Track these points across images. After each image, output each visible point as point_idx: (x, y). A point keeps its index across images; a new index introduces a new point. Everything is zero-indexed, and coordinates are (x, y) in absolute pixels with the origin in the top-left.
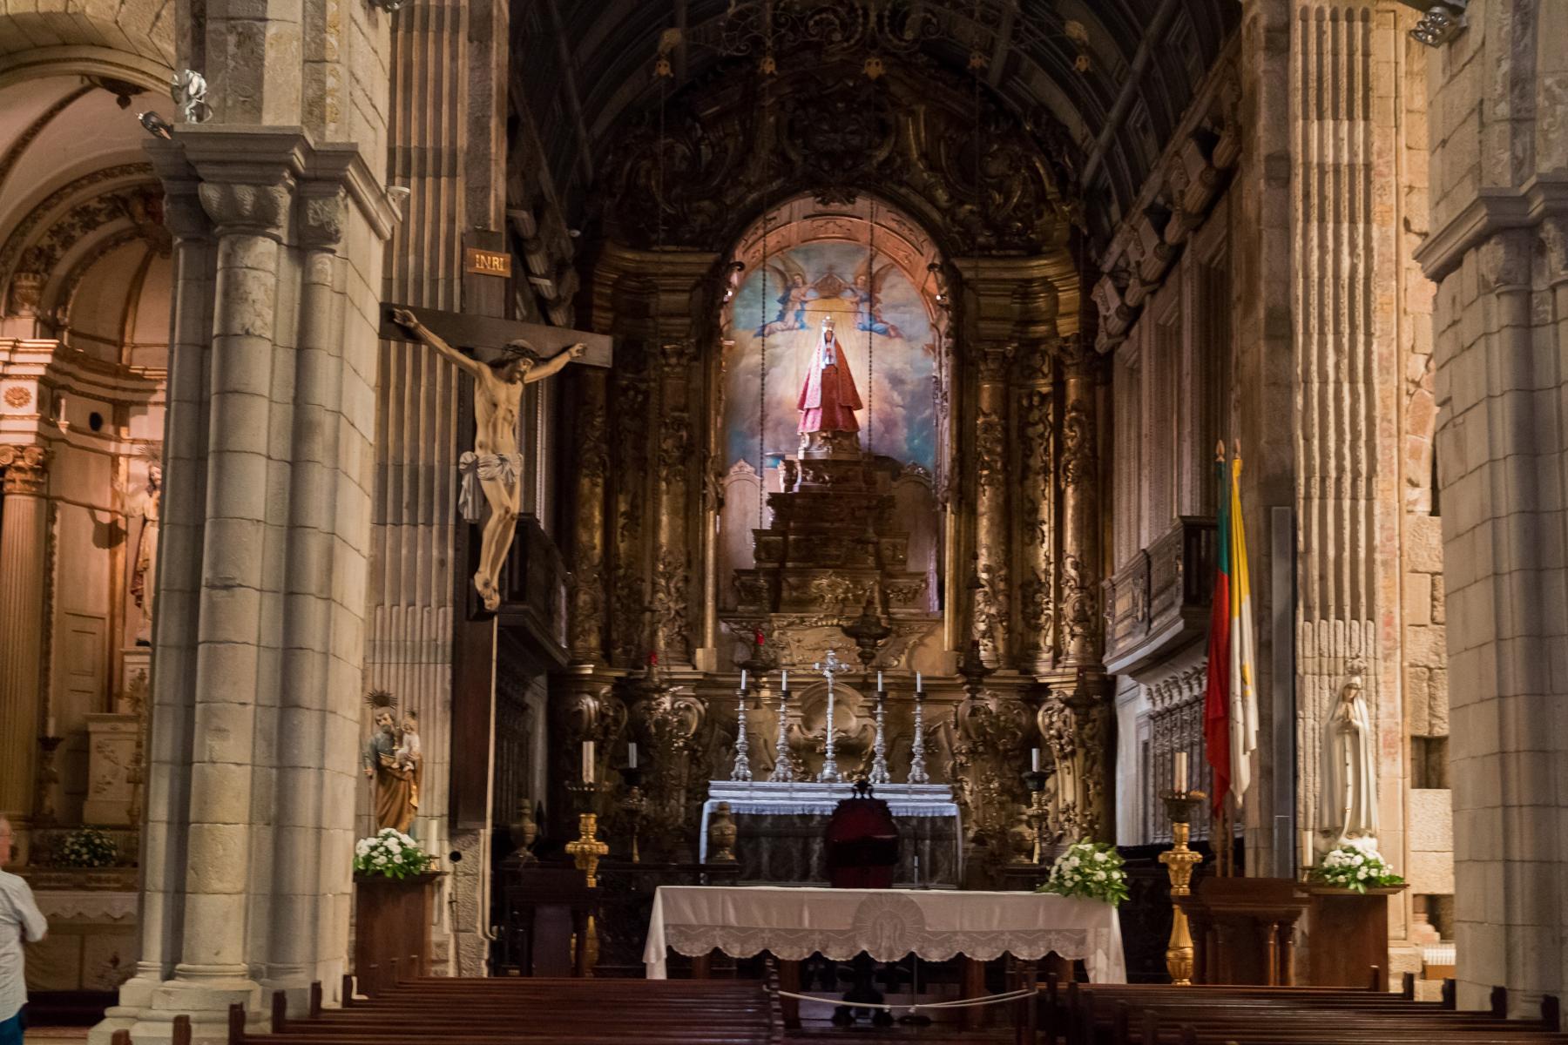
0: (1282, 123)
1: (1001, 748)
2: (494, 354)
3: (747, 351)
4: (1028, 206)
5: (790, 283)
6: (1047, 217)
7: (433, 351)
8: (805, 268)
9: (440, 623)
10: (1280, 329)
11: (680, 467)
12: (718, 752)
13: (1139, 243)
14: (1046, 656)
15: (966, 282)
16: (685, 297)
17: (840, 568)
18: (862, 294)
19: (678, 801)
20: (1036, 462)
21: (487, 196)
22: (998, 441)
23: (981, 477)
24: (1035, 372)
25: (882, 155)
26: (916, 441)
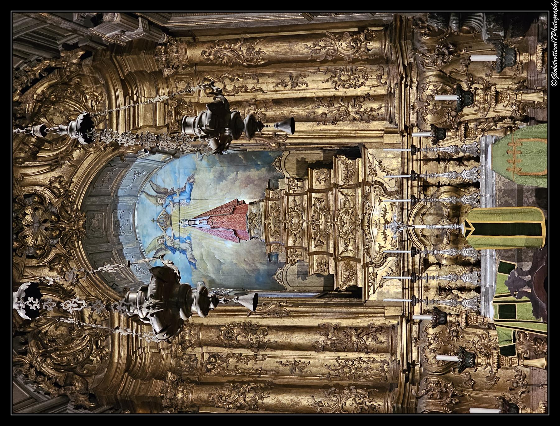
3: (205, 274)
5: (163, 246)
8: (154, 237)
18: (168, 200)
26: (259, 163)
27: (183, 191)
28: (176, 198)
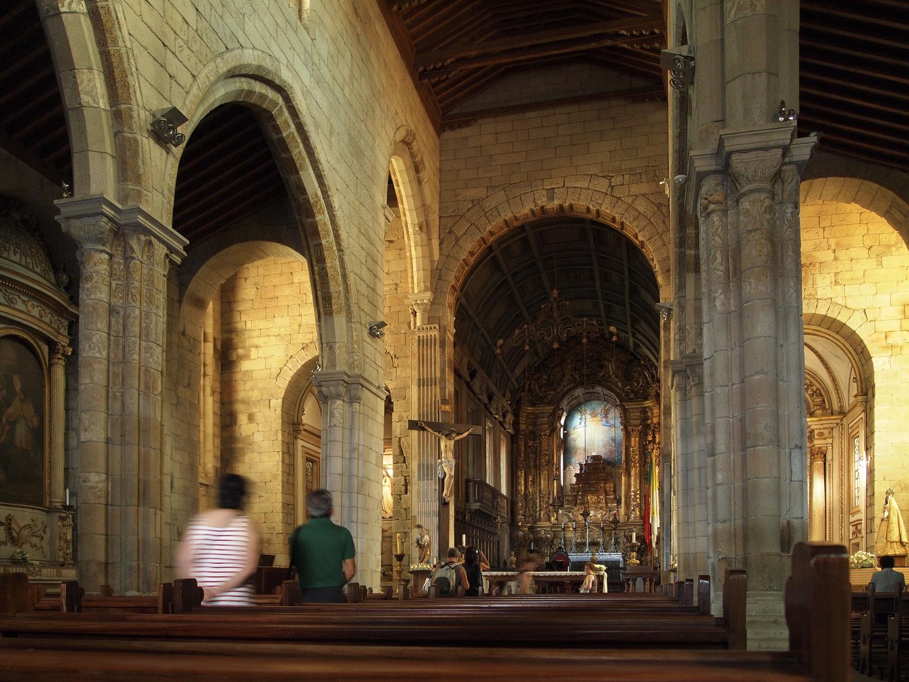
7: (431, 433)
15: (626, 409)
21: (445, 390)
25: (602, 374)
27: (607, 422)
28: (604, 419)
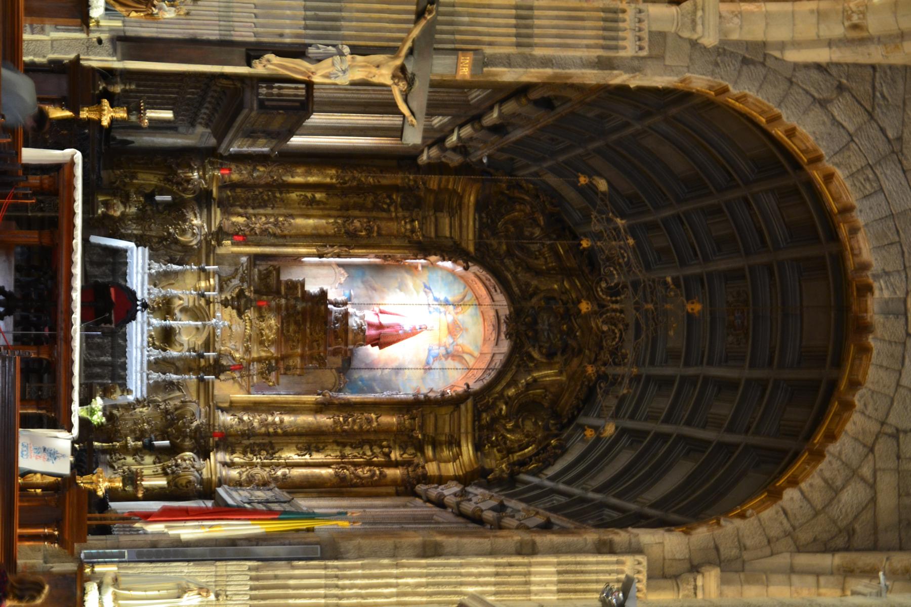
0: (556, 551)
1: (169, 430)
2: (410, 68)
4: (505, 443)
6: (498, 455)
7: (409, 31)
9: (244, 33)
10: (430, 551)
11: (343, 231)
12: (166, 255)
13: (484, 501)
14: (228, 458)
16: (448, 234)
17: (281, 332)
18: (451, 349)
19: (135, 229)
20: (348, 451)
21: (504, 66)
22: (361, 427)
23: (338, 416)
24: (404, 449)
25: (536, 355)
26: (360, 383)
27: (436, 358)
28: (442, 351)
